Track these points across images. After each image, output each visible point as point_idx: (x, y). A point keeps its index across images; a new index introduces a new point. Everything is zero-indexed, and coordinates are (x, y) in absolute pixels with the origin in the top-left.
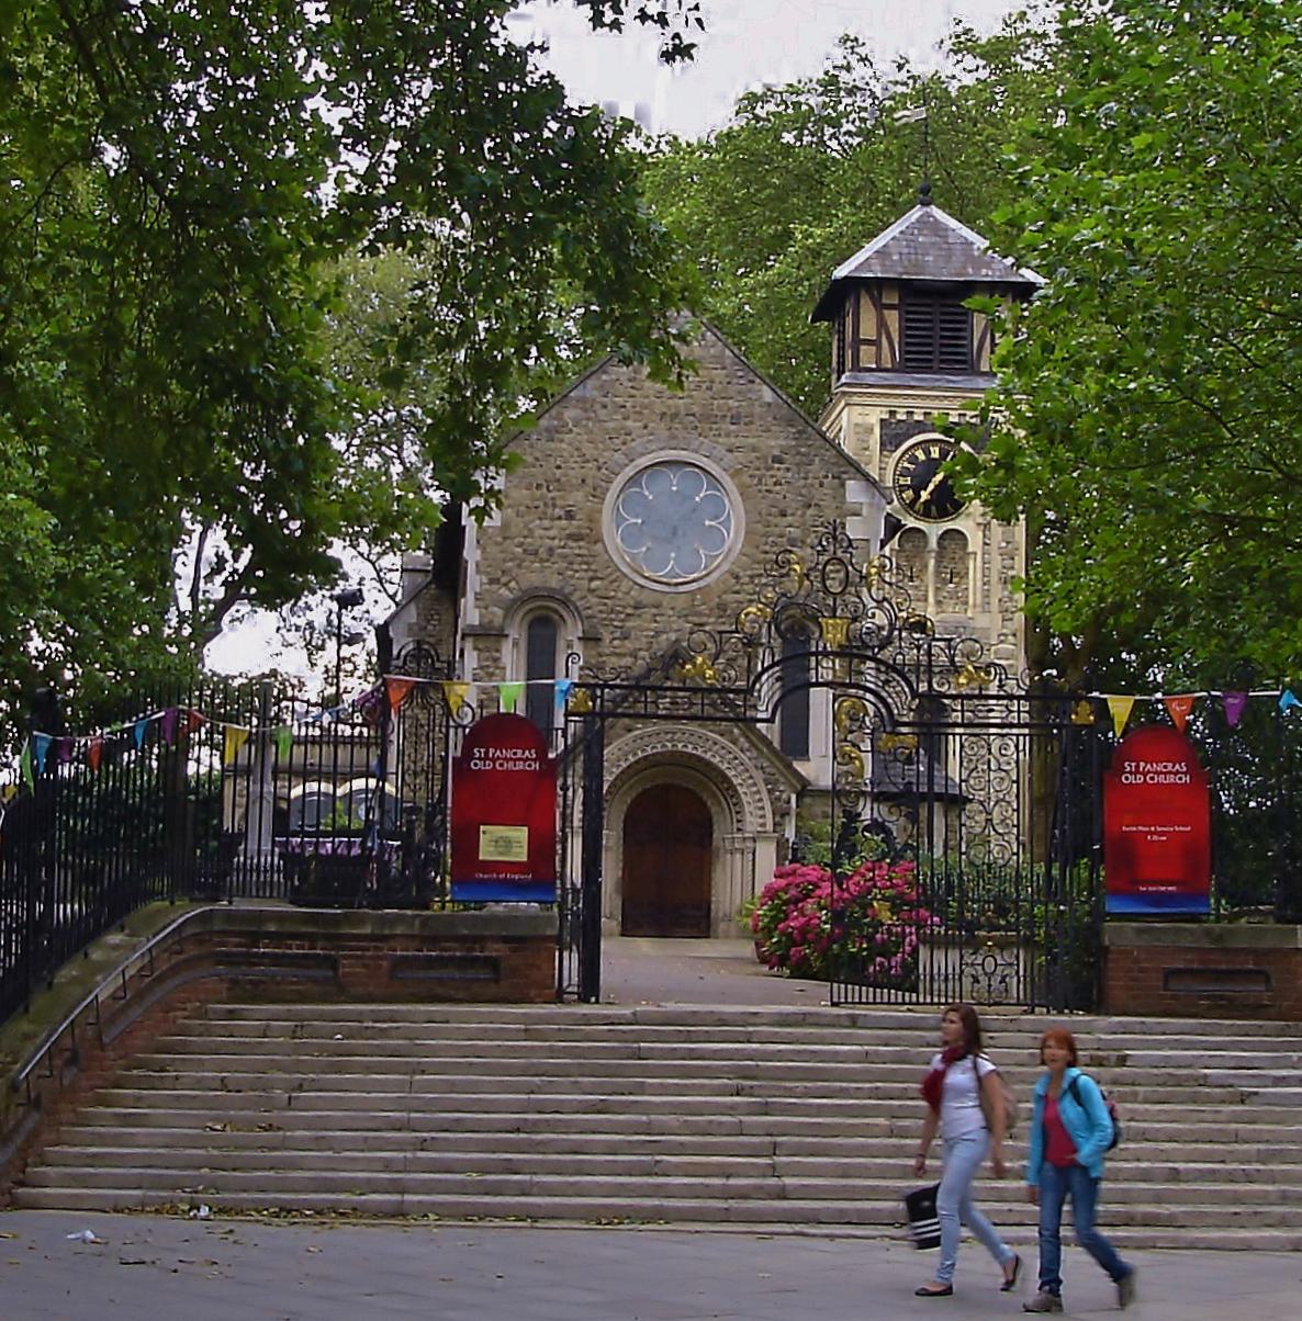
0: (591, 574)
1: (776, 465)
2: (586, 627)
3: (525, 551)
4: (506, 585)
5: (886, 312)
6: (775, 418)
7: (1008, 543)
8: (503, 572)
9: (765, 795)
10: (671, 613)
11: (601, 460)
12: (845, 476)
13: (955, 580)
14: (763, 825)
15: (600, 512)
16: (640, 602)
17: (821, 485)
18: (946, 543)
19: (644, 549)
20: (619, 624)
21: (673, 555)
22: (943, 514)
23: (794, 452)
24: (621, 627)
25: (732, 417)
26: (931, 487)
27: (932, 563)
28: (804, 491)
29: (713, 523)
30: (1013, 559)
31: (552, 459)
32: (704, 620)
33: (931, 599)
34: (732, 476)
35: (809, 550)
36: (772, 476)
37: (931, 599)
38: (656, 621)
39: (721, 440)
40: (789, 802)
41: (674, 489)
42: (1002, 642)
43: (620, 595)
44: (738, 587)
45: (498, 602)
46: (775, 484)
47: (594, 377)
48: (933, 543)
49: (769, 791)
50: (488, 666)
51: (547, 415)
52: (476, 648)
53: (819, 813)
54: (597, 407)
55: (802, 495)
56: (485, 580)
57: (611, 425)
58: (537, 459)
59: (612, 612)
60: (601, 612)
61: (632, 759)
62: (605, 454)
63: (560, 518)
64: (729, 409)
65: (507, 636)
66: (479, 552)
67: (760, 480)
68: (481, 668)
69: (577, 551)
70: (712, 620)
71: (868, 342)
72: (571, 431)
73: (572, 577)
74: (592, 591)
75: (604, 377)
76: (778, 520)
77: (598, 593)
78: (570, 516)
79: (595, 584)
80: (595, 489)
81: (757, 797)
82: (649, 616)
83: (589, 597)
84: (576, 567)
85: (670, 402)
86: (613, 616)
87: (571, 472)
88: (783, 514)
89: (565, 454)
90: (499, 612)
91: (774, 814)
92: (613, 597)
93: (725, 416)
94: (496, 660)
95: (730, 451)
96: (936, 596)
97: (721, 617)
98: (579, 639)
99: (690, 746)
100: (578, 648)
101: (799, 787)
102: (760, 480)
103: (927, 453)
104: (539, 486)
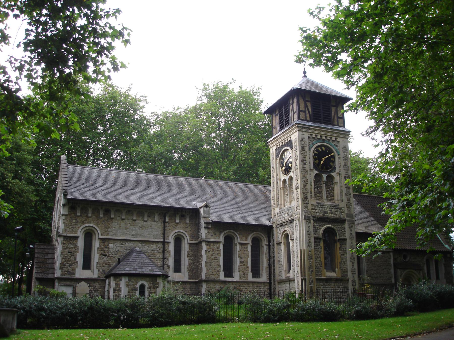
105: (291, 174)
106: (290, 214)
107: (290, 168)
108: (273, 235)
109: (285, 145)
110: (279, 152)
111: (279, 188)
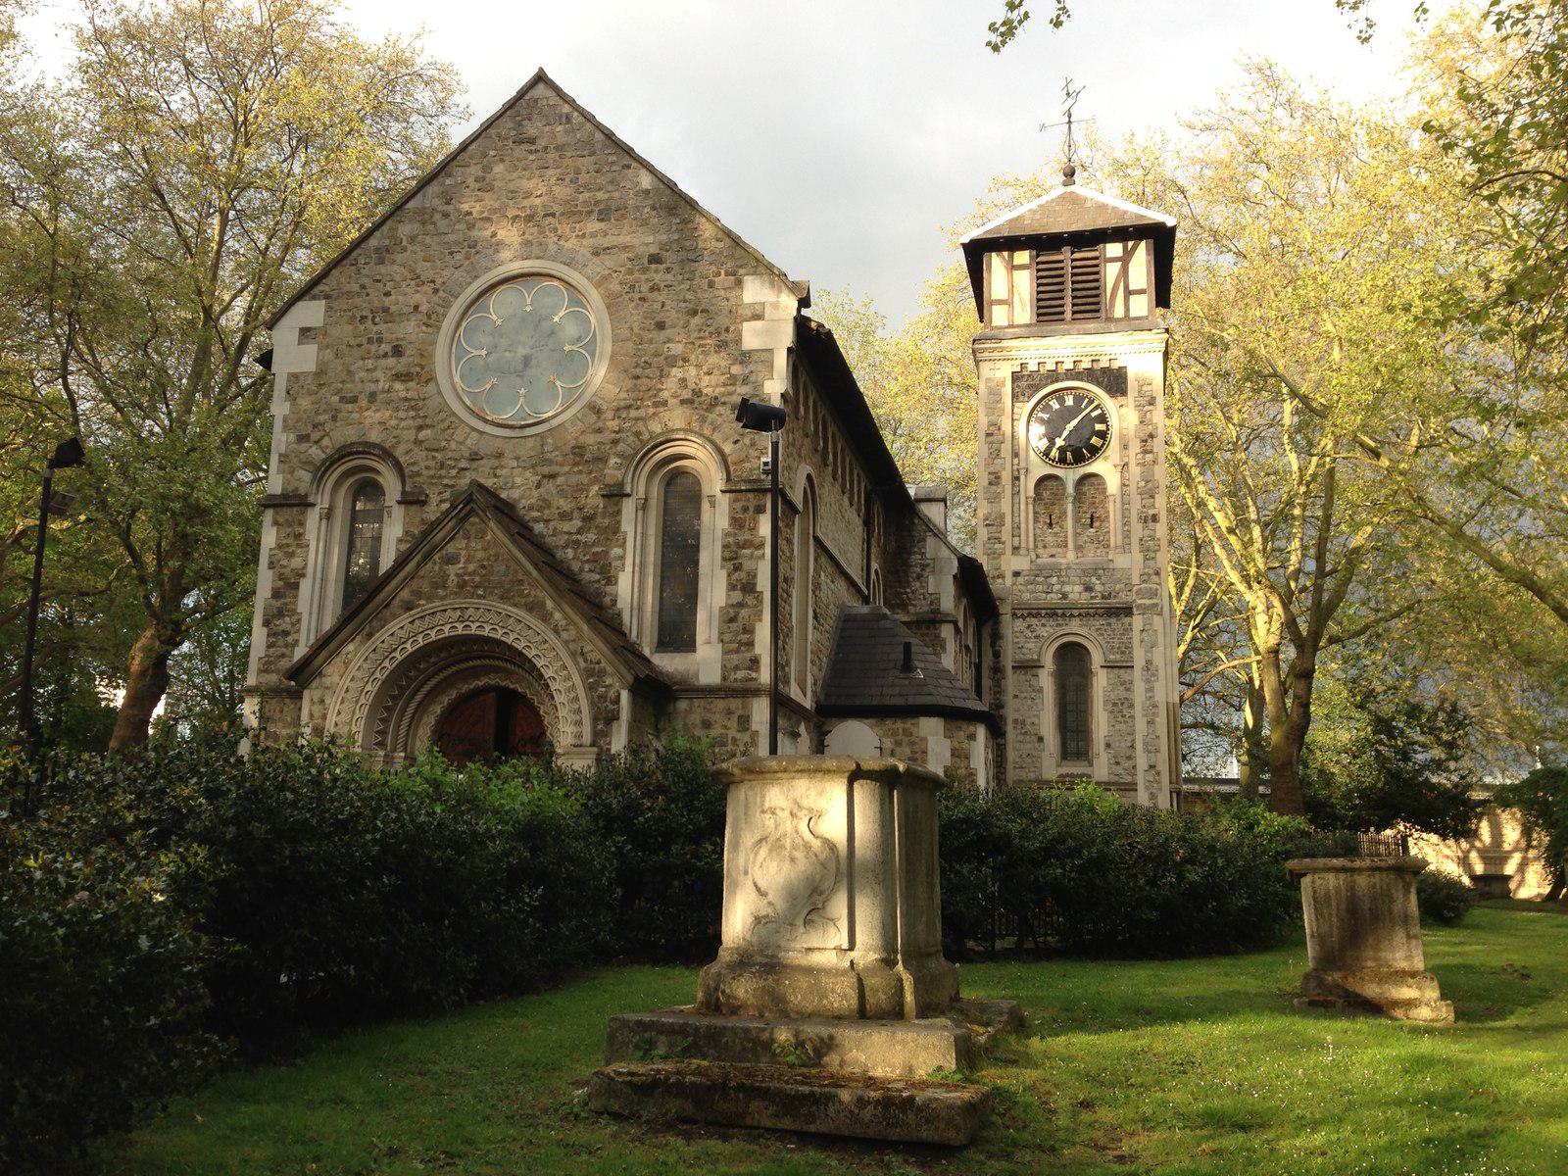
0: (419, 421)
1: (653, 266)
2: (408, 489)
3: (343, 399)
4: (316, 442)
5: (1016, 273)
6: (654, 208)
7: (1147, 482)
8: (315, 426)
9: (581, 693)
10: (515, 464)
11: (439, 281)
12: (741, 271)
13: (1096, 524)
14: (580, 736)
15: (434, 343)
16: (477, 454)
17: (711, 285)
18: (1085, 489)
19: (488, 386)
20: (451, 483)
21: (523, 391)
22: (1079, 459)
23: (675, 247)
24: (453, 486)
25: (600, 212)
26: (1066, 433)
27: (1070, 507)
28: (689, 296)
29: (575, 348)
30: (1153, 497)
31: (380, 285)
32: (555, 469)
33: (1071, 545)
34: (598, 285)
35: (693, 372)
36: (647, 280)
37: (1071, 545)
38: (495, 476)
39: (585, 242)
40: (617, 700)
41: (528, 309)
42: (1144, 581)
43: (453, 445)
44: (600, 424)
45: (307, 463)
46: (652, 289)
47: (435, 182)
48: (1070, 489)
49: (591, 688)
50: (288, 545)
51: (377, 234)
52: (276, 523)
53: (698, 722)
54: (437, 216)
55: (685, 301)
56: (292, 437)
57: (452, 238)
58: (363, 287)
59: (442, 466)
60: (427, 468)
61: (410, 648)
62: (444, 273)
63: (385, 355)
64: (597, 203)
65: (313, 505)
66: (288, 404)
67: (632, 287)
68: (280, 546)
69: (403, 394)
70: (566, 469)
71: (1000, 302)
72: (405, 249)
73: (396, 428)
74: (417, 442)
75: (448, 182)
76: (654, 334)
77: (426, 445)
78: (397, 351)
79: (422, 435)
80: (429, 317)
81: (573, 695)
82: (487, 470)
83: (416, 450)
84: (402, 414)
85: (526, 203)
86: (443, 472)
87: (400, 298)
88: (661, 326)
89: (398, 278)
90: (306, 476)
91: (595, 720)
92: (444, 449)
93: (592, 212)
94: (299, 536)
95: (596, 254)
96: (1075, 540)
97: (577, 464)
98: (399, 502)
99: (488, 628)
100: (398, 512)
101: (630, 679)
102: (632, 287)
103: (1061, 401)
104: (363, 318)
105: (1097, 467)
106: (1099, 588)
107: (1094, 451)
108: (996, 636)
109: (1091, 375)
110: (1037, 388)
111: (1023, 500)
